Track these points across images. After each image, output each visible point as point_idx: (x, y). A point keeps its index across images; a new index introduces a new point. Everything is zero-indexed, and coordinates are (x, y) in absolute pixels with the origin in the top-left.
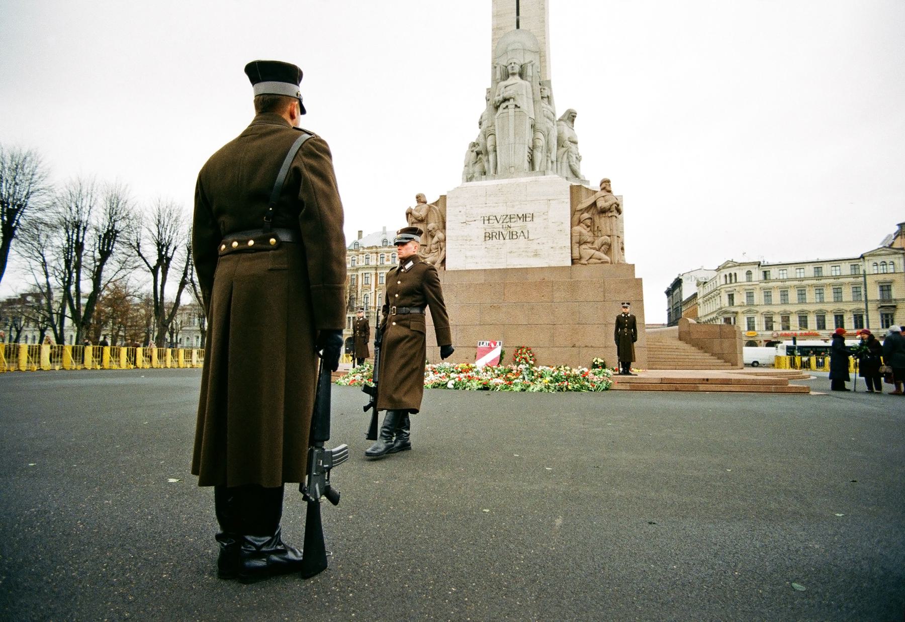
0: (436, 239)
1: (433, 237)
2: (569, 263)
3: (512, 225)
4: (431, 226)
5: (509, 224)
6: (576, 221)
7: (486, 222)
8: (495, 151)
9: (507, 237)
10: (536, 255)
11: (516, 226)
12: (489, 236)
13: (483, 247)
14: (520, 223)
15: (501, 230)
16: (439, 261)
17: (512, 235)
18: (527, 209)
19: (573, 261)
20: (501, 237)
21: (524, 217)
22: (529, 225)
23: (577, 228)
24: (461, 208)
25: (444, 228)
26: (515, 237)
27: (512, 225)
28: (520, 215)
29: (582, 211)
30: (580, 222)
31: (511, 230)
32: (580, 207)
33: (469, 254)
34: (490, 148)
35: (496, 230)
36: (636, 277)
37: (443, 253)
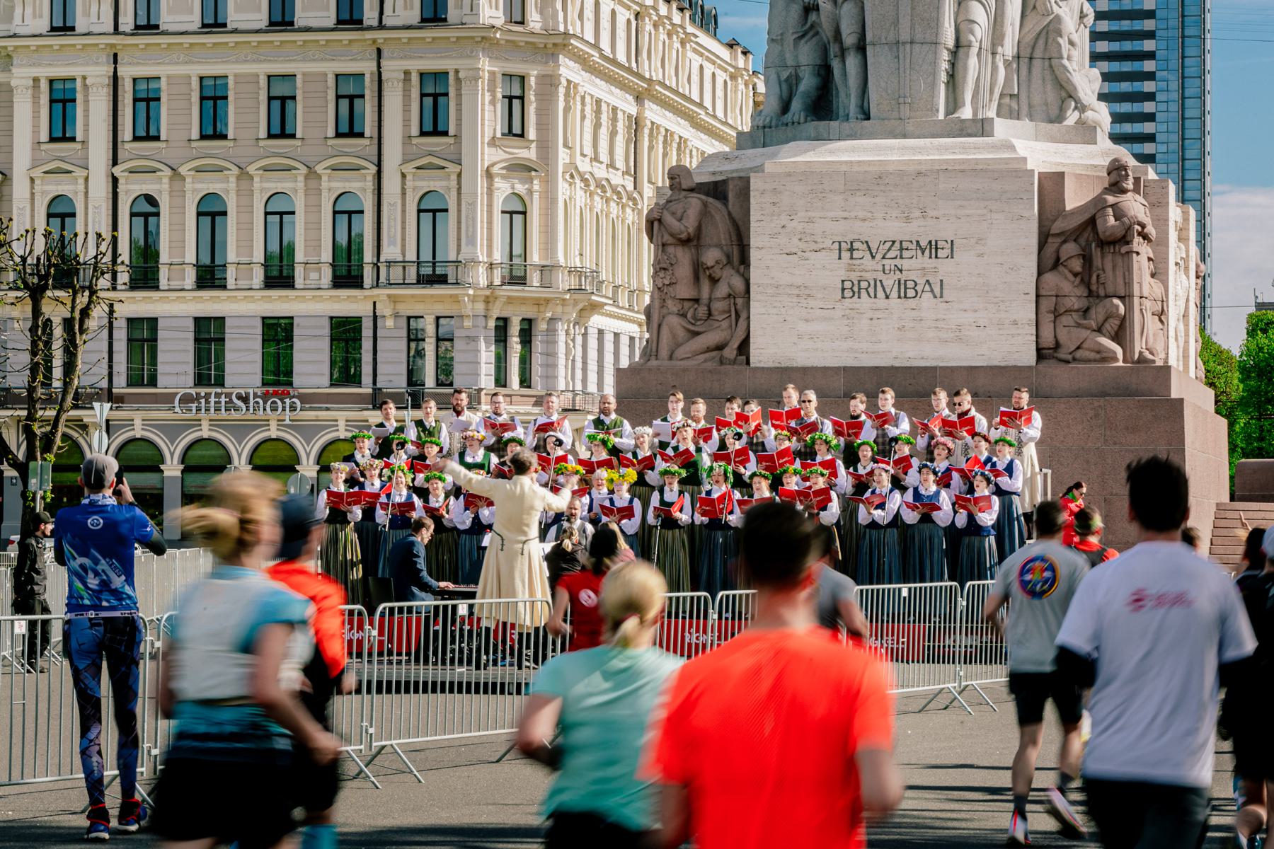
0: (722, 290)
1: (714, 281)
2: (1028, 357)
3: (905, 264)
4: (711, 256)
5: (898, 262)
6: (1048, 263)
7: (846, 255)
8: (861, 48)
9: (894, 294)
10: (959, 339)
11: (915, 265)
12: (851, 289)
13: (838, 313)
14: (924, 261)
15: (880, 276)
16: (735, 344)
17: (904, 290)
18: (943, 231)
19: (1041, 354)
20: (880, 294)
21: (934, 247)
22: (944, 267)
23: (1050, 278)
24: (784, 220)
25: (745, 260)
26: (911, 293)
27: (905, 264)
28: (924, 243)
29: (1066, 237)
30: (1057, 263)
31: (903, 277)
32: (1057, 227)
33: (802, 327)
34: (849, 39)
36: (1174, 396)
37: (742, 322)
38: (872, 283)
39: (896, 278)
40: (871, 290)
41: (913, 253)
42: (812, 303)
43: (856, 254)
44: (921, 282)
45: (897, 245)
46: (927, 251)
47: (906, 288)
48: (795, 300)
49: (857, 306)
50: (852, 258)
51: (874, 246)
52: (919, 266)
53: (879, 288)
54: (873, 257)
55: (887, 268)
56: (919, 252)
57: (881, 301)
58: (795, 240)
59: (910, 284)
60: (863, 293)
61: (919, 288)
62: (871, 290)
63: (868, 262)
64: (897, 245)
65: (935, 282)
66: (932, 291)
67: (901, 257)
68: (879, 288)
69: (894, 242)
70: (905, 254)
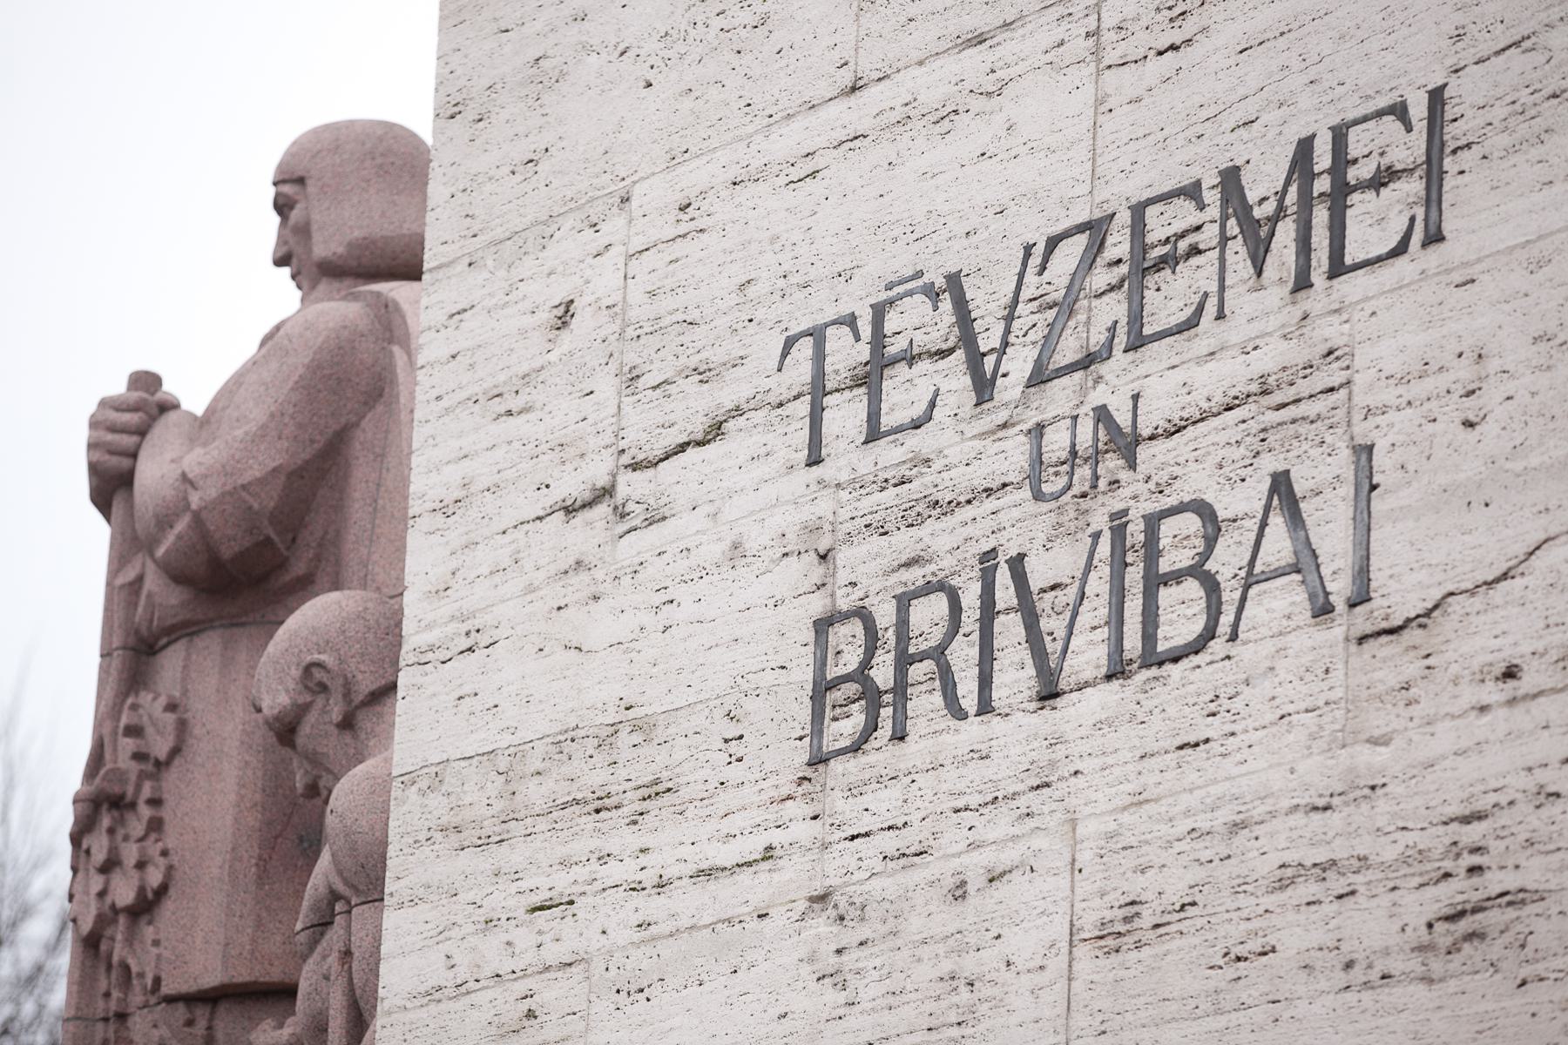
3: (1155, 385)
7: (845, 415)
28: (1264, 183)
35: (949, 544)
38: (971, 599)
39: (1100, 521)
40: (964, 655)
41: (1195, 277)
42: (675, 842)
43: (903, 394)
44: (1241, 500)
45: (1118, 244)
46: (1286, 232)
47: (1155, 582)
48: (585, 837)
49: (885, 802)
50: (874, 433)
51: (986, 305)
52: (1232, 373)
53: (1009, 629)
54: (984, 387)
55: (1057, 442)
56: (1238, 253)
57: (1017, 733)
58: (607, 386)
59: (1179, 542)
60: (925, 703)
61: (1227, 561)
62: (964, 655)
63: (965, 448)
64: (1118, 244)
65: (1321, 471)
66: (1305, 562)
67: (1137, 342)
68: (1009, 629)
69: (1096, 229)
70: (1168, 299)
